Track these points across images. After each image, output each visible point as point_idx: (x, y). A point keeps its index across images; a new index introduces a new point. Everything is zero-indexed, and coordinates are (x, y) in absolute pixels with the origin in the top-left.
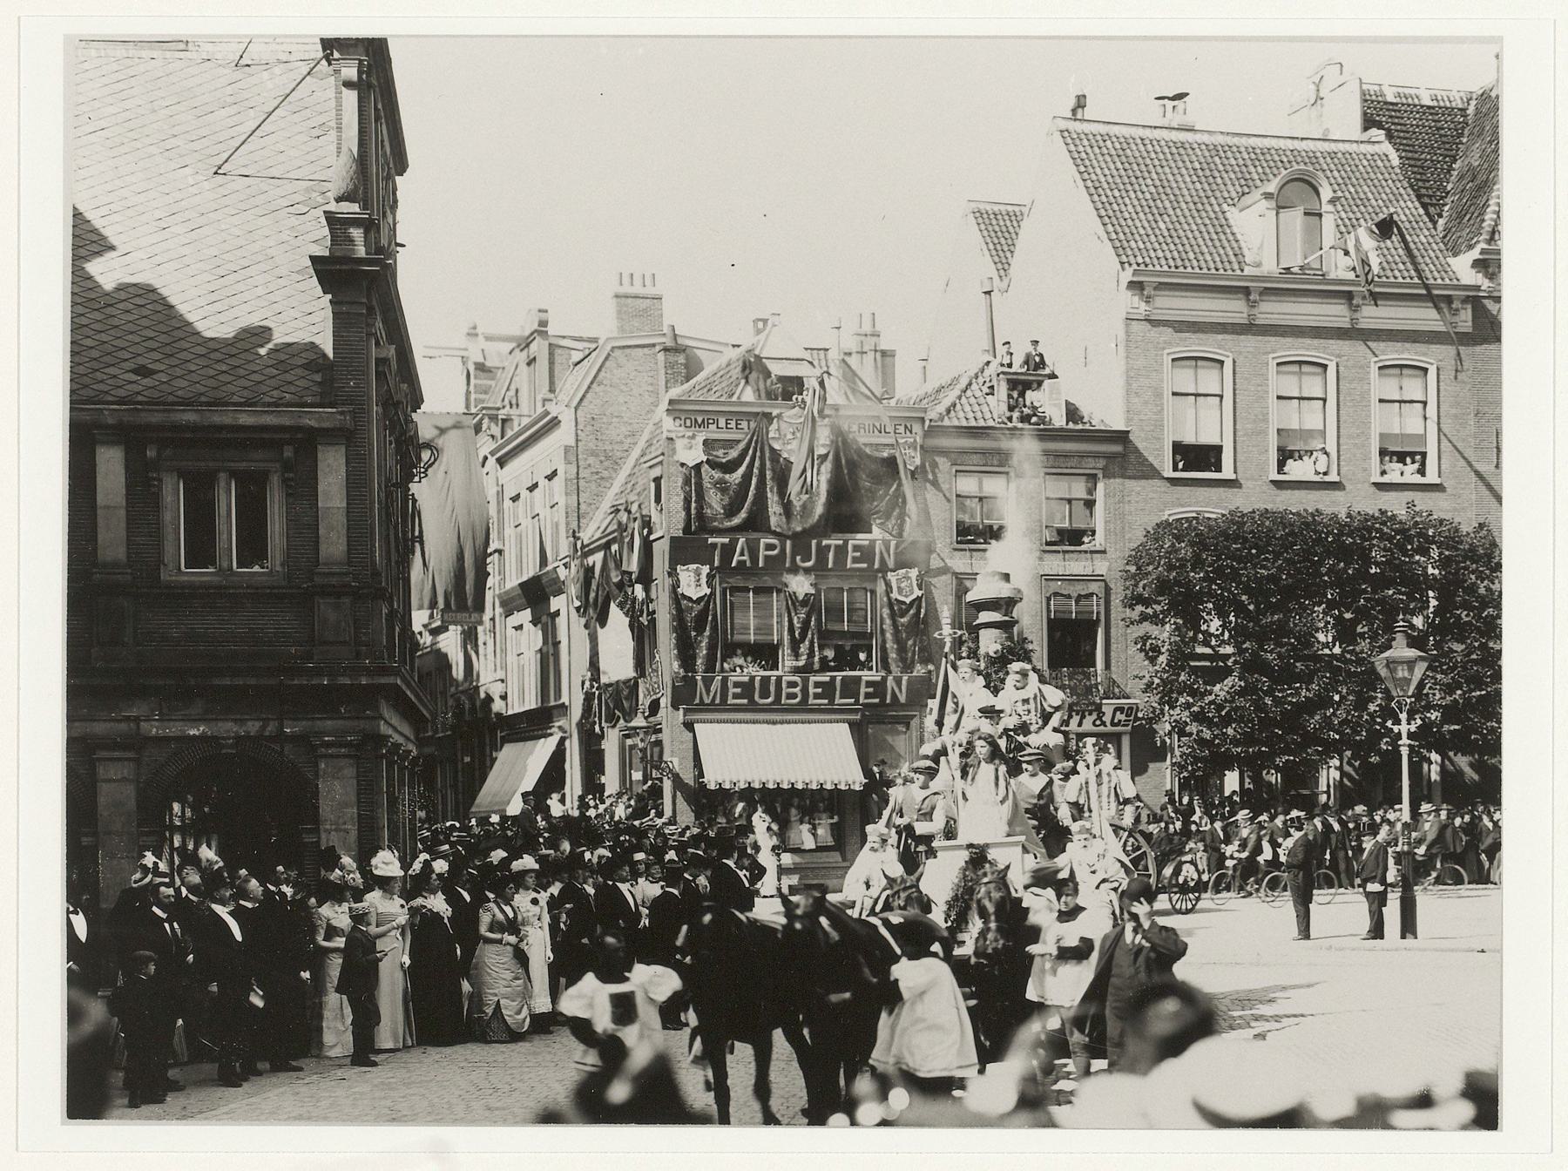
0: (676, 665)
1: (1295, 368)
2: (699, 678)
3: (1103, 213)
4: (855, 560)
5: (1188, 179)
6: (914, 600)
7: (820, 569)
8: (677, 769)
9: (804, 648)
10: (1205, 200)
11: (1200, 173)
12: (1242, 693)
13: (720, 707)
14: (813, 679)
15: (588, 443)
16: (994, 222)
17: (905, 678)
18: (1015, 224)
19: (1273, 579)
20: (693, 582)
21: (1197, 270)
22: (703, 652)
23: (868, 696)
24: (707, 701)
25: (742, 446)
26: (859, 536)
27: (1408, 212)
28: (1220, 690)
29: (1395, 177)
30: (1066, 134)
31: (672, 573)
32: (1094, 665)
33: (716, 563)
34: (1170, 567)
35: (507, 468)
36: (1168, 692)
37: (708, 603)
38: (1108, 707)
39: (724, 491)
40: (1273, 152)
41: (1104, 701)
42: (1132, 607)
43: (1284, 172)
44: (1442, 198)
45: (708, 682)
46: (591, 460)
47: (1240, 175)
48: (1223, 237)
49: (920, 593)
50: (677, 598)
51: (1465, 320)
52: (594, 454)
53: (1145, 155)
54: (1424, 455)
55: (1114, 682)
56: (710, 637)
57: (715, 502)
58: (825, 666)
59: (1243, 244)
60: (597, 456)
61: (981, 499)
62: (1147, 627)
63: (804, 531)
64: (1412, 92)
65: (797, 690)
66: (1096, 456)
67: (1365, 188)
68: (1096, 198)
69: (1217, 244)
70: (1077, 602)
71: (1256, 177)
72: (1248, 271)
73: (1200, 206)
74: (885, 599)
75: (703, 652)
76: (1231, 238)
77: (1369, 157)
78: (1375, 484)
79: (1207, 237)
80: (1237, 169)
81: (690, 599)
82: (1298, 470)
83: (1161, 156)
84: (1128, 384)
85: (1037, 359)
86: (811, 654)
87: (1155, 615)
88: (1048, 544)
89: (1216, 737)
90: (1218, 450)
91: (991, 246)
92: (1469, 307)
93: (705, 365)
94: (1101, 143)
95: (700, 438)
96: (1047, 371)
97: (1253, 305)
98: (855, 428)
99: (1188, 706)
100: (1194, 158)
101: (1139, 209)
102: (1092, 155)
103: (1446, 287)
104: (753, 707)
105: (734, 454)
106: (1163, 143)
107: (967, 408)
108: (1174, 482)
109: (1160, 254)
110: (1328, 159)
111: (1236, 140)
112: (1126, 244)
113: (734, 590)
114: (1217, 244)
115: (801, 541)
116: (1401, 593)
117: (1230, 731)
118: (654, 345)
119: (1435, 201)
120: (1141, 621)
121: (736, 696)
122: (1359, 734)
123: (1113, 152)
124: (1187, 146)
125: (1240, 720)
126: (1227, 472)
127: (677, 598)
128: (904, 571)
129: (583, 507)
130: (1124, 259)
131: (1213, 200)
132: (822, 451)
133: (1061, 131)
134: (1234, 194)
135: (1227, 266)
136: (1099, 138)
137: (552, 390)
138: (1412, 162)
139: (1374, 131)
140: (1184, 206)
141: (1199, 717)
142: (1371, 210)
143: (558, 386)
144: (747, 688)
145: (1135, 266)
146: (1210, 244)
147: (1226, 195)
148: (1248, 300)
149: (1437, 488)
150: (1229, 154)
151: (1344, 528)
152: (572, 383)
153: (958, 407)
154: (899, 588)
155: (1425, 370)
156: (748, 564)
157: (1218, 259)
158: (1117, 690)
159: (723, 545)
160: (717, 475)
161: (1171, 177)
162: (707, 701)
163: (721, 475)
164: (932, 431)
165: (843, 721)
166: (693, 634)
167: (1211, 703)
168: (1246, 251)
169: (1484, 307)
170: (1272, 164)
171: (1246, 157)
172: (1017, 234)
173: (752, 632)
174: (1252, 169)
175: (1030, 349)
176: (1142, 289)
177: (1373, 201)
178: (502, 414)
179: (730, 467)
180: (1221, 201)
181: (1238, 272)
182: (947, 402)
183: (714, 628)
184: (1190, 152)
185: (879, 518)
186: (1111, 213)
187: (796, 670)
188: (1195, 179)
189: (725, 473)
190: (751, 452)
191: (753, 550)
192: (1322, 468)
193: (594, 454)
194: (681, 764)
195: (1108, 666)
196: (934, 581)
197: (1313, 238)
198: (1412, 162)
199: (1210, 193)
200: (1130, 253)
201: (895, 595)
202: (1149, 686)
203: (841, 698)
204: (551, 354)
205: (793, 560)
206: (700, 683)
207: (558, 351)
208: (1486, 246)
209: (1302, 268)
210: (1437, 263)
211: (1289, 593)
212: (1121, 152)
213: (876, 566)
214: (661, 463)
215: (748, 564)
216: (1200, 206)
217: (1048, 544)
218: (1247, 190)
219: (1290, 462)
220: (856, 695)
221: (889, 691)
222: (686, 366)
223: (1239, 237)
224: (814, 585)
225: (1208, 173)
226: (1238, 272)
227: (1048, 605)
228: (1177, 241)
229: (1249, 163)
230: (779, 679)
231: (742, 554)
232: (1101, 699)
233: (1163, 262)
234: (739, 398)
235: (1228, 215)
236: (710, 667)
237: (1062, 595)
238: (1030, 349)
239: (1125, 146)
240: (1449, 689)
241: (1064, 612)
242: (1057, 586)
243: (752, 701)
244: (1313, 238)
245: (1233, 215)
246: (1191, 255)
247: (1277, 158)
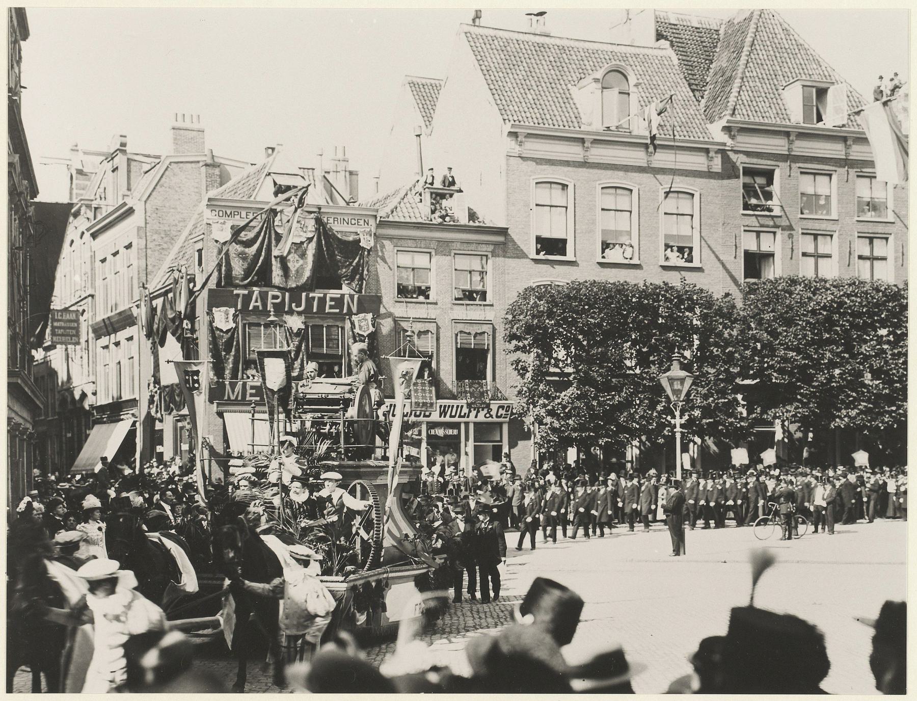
0: (211, 374)
1: (613, 191)
2: (227, 383)
3: (492, 87)
4: (331, 307)
5: (546, 67)
7: (308, 312)
8: (212, 443)
10: (557, 82)
11: (554, 64)
12: (579, 398)
15: (153, 225)
16: (422, 90)
18: (436, 91)
19: (599, 325)
20: (224, 319)
21: (552, 126)
22: (230, 365)
24: (233, 398)
25: (257, 230)
26: (332, 291)
27: (683, 95)
28: (566, 395)
29: (675, 72)
30: (468, 35)
31: (210, 313)
32: (485, 378)
33: (239, 307)
34: (533, 317)
35: (97, 240)
36: (532, 396)
38: (494, 407)
39: (244, 259)
40: (600, 52)
41: (492, 402)
42: (510, 342)
43: (606, 66)
44: (704, 86)
45: (233, 386)
46: (155, 237)
47: (579, 67)
48: (568, 105)
49: (374, 330)
50: (212, 330)
51: (717, 165)
52: (157, 232)
53: (519, 50)
54: (691, 249)
55: (498, 389)
56: (235, 356)
57: (238, 268)
59: (580, 110)
60: (160, 234)
61: (413, 269)
62: (519, 354)
63: (297, 287)
64: (687, 17)
66: (487, 243)
67: (657, 78)
68: (487, 77)
69: (565, 110)
70: (475, 337)
71: (589, 68)
73: (553, 85)
74: (351, 333)
75: (230, 365)
76: (573, 106)
77: (659, 58)
78: (661, 266)
79: (558, 105)
80: (577, 62)
81: (221, 331)
82: (614, 256)
83: (529, 52)
84: (508, 198)
85: (451, 179)
87: (525, 346)
88: (456, 299)
89: (562, 426)
90: (564, 241)
91: (421, 106)
92: (719, 156)
93: (232, 177)
94: (491, 42)
95: (230, 223)
96: (456, 188)
97: (587, 150)
98: (331, 220)
99: (544, 406)
100: (550, 54)
101: (515, 85)
102: (485, 50)
103: (706, 143)
106: (530, 43)
107: (405, 210)
108: (536, 261)
109: (528, 115)
110: (634, 58)
111: (577, 44)
112: (506, 108)
113: (251, 325)
114: (565, 110)
115: (295, 293)
116: (676, 336)
117: (571, 422)
118: (198, 162)
119: (699, 88)
120: (515, 351)
121: (252, 395)
122: (651, 424)
123: (499, 48)
124: (546, 46)
125: (578, 415)
126: (569, 257)
127: (212, 330)
128: (362, 315)
129: (150, 268)
130: (506, 117)
131: (562, 82)
132: (310, 235)
133: (466, 33)
134: (575, 79)
135: (571, 124)
136: (490, 38)
137: (129, 189)
138: (686, 63)
139: (662, 41)
140: (543, 85)
141: (551, 413)
142: (660, 92)
143: (133, 187)
145: (512, 122)
146: (560, 110)
147: (570, 78)
148: (584, 146)
149: (699, 270)
150: (572, 52)
151: (644, 294)
152: (142, 185)
153: (399, 209)
155: (693, 195)
156: (261, 308)
157: (564, 120)
158: (499, 395)
159: (244, 295)
160: (240, 248)
161: (535, 66)
162: (233, 398)
163: (243, 249)
164: (382, 224)
166: (223, 353)
167: (559, 404)
168: (582, 115)
169: (728, 156)
170: (599, 60)
171: (583, 55)
172: (437, 98)
174: (586, 62)
175: (447, 172)
176: (517, 137)
177: (662, 87)
178: (94, 205)
179: (248, 244)
180: (567, 82)
181: (578, 129)
182: (391, 206)
183: (237, 350)
184: (548, 50)
185: (347, 280)
186: (497, 87)
188: (550, 67)
189: (245, 247)
190: (262, 234)
191: (263, 297)
192: (628, 254)
193: (157, 232)
194: (214, 440)
195: (494, 379)
196: (382, 321)
197: (625, 111)
198: (686, 63)
199: (560, 77)
200: (509, 113)
201: (357, 330)
202: (520, 392)
204: (129, 165)
206: (228, 387)
207: (133, 164)
208: (730, 118)
209: (617, 127)
210: (700, 127)
211: (608, 335)
212: (504, 48)
213: (345, 311)
214: (202, 239)
215: (261, 308)
216: (553, 85)
217: (456, 299)
218: (583, 76)
219: (607, 251)
222: (220, 176)
223: (578, 106)
224: (305, 323)
225: (559, 64)
226: (578, 129)
227: (456, 339)
228: (539, 107)
229: (585, 59)
231: (256, 301)
232: (490, 400)
233: (530, 119)
235: (571, 92)
236: (234, 375)
237: (465, 333)
238: (447, 172)
239: (506, 44)
240: (705, 397)
241: (467, 344)
242: (460, 327)
244: (625, 111)
245: (574, 90)
246: (548, 117)
247: (602, 56)
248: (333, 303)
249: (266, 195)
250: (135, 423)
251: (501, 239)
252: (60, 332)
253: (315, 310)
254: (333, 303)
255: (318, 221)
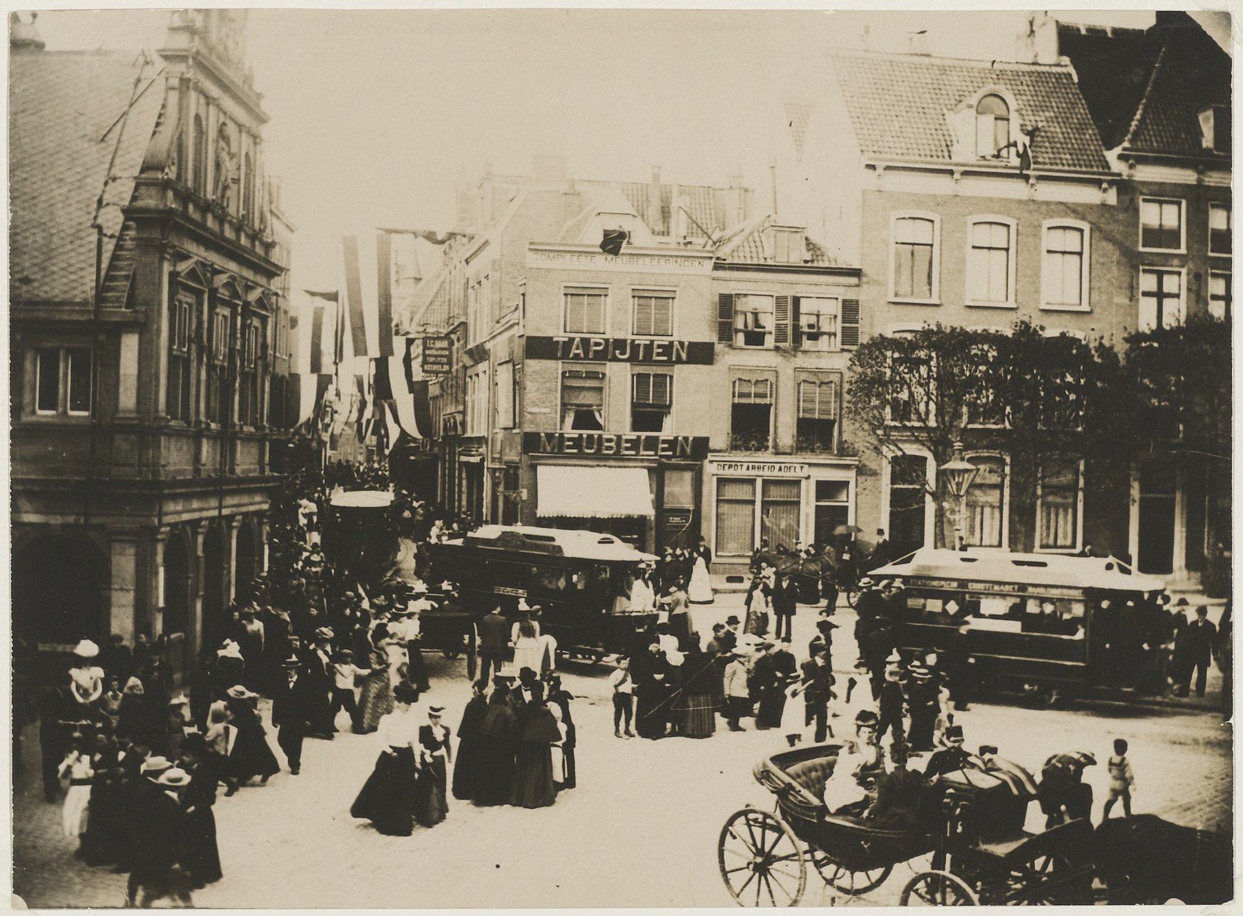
4: (659, 354)
23: (664, 450)
65: (612, 444)
72: (954, 159)
104: (581, 456)
165: (644, 467)
168: (955, 143)
181: (947, 160)
203: (645, 450)
205: (614, 354)
235: (946, 117)
242: (804, 376)
243: (581, 450)
248: (660, 350)
251: (854, 280)
252: (432, 359)
253: (641, 358)
254: (660, 350)
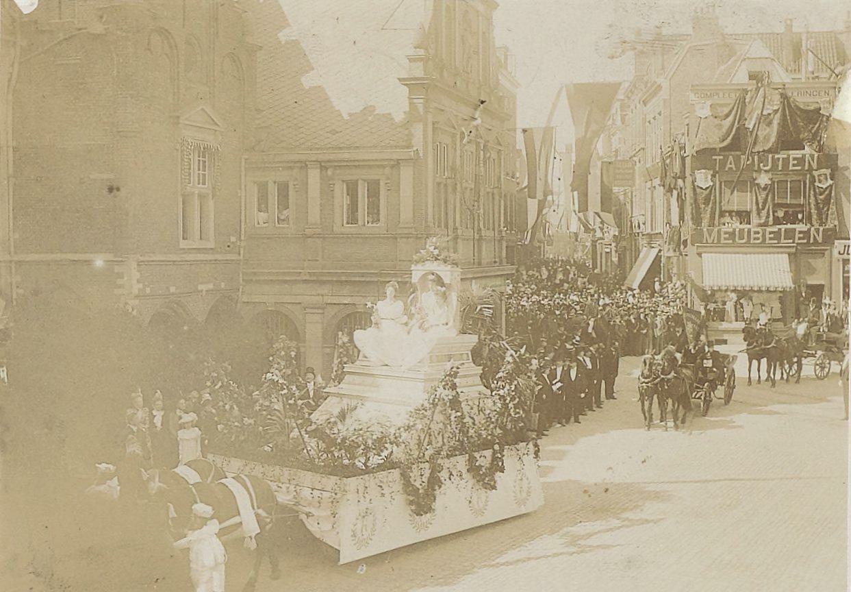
2: (705, 230)
4: (794, 165)
6: (828, 187)
8: (693, 278)
9: (764, 213)
13: (717, 245)
14: (769, 229)
17: (821, 229)
25: (731, 106)
31: (692, 174)
37: (711, 191)
58: (777, 221)
65: (759, 236)
86: (768, 217)
95: (709, 103)
98: (795, 94)
104: (734, 245)
105: (726, 110)
144: (732, 235)
154: (819, 180)
156: (734, 169)
159: (720, 159)
173: (735, 204)
187: (760, 225)
213: (806, 168)
215: (734, 169)
220: (794, 238)
221: (812, 234)
230: (749, 231)
234: (731, 81)
236: (711, 224)
249: (742, 78)
250: (660, 251)
255: (784, 97)
